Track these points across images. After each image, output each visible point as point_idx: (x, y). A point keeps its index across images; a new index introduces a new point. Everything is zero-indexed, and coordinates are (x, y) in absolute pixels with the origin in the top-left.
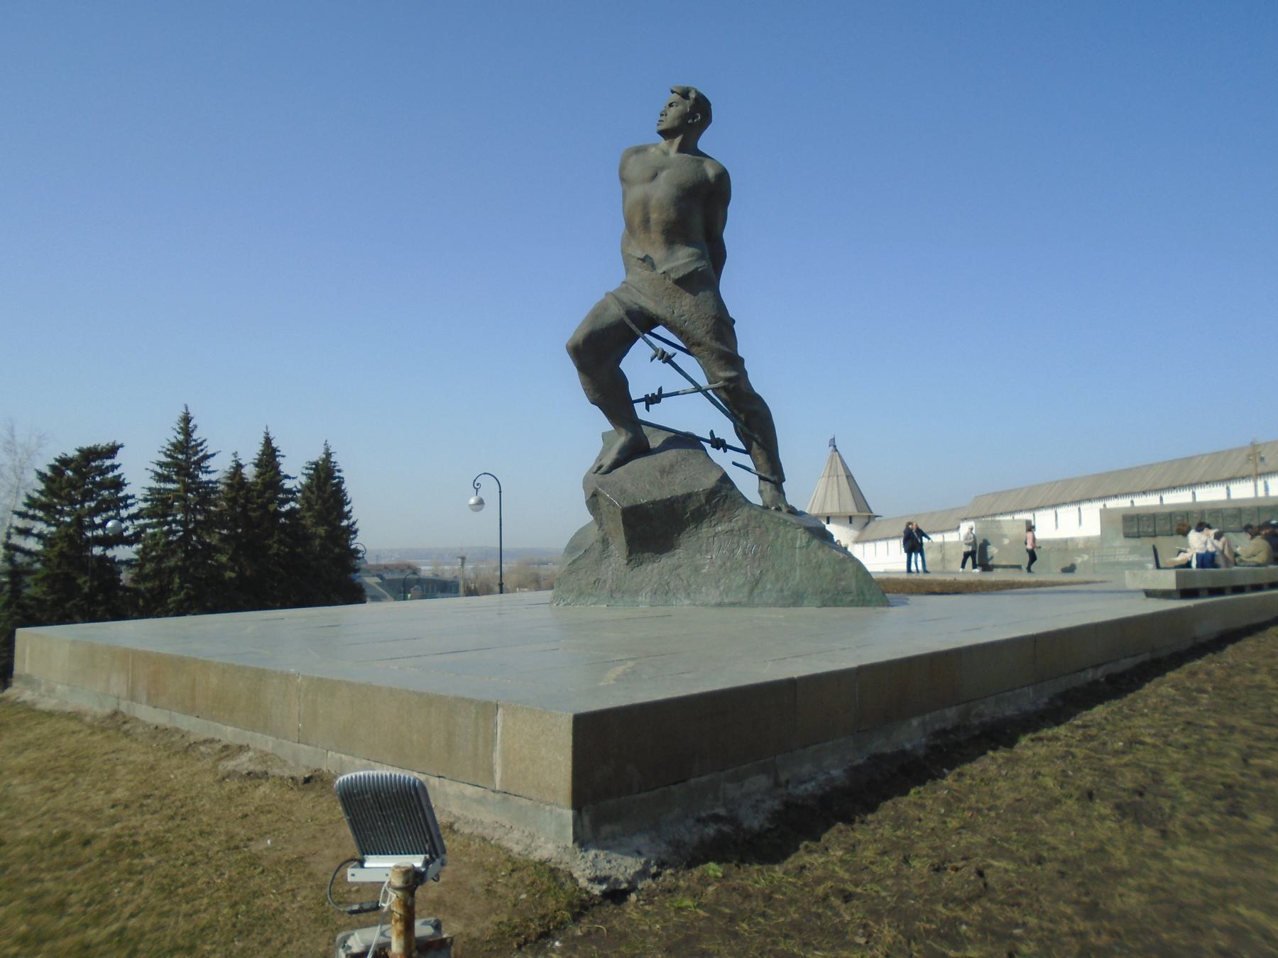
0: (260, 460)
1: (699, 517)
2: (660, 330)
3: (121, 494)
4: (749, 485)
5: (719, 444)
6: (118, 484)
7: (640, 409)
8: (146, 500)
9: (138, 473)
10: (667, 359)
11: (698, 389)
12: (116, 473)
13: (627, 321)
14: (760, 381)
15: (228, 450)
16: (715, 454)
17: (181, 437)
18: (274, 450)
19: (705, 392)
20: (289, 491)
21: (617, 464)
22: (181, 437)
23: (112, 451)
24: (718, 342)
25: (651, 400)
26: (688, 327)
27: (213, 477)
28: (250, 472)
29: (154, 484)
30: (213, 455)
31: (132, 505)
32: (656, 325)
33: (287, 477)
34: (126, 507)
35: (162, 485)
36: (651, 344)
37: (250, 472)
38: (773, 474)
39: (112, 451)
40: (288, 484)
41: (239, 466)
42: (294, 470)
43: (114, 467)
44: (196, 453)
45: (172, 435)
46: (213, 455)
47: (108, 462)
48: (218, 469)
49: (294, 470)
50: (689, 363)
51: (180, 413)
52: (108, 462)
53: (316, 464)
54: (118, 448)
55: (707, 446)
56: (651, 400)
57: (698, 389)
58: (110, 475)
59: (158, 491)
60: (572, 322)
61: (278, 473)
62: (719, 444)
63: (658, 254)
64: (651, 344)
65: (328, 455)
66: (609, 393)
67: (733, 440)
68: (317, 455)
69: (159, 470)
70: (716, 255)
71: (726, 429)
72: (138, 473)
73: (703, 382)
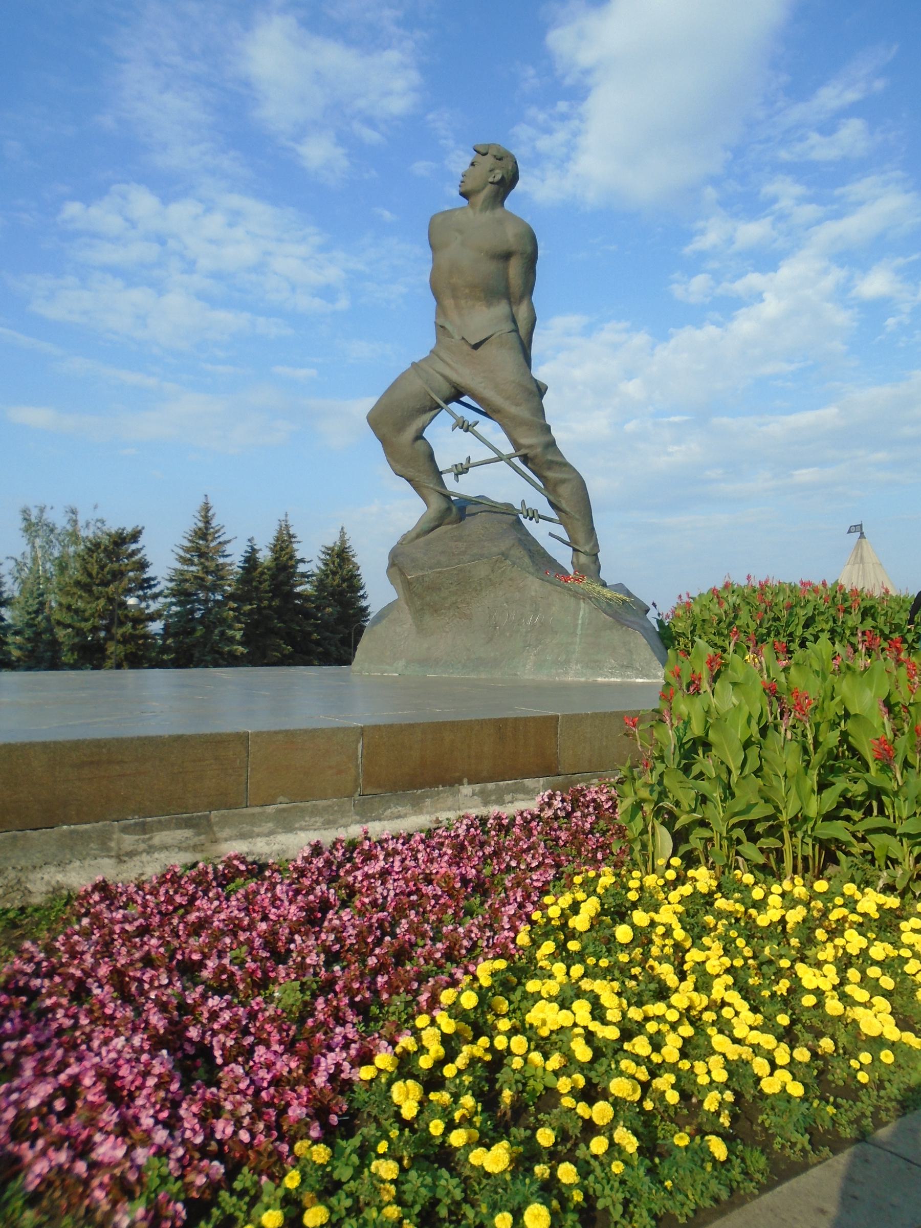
0: (275, 546)
2: (466, 399)
3: (145, 576)
5: (533, 515)
6: (143, 566)
8: (171, 580)
9: (163, 558)
11: (500, 458)
12: (140, 556)
13: (429, 390)
15: (245, 535)
17: (201, 525)
18: (291, 536)
19: (508, 459)
20: (304, 575)
21: (418, 536)
22: (201, 525)
23: (135, 536)
25: (461, 470)
26: (489, 394)
27: (228, 560)
28: (265, 556)
29: (178, 566)
30: (229, 541)
31: (155, 585)
32: (462, 395)
33: (302, 561)
34: (150, 587)
35: (186, 568)
36: (452, 414)
37: (265, 556)
39: (135, 536)
40: (301, 568)
41: (254, 551)
42: (310, 556)
43: (139, 550)
44: (215, 538)
45: (192, 522)
46: (229, 541)
47: (133, 547)
48: (235, 557)
49: (310, 556)
51: (199, 503)
52: (133, 547)
53: (332, 549)
54: (140, 532)
55: (521, 516)
56: (461, 470)
58: (136, 558)
59: (182, 573)
61: (292, 557)
62: (533, 515)
64: (452, 414)
65: (343, 542)
66: (417, 465)
68: (332, 540)
69: (182, 554)
72: (163, 558)
73: (507, 449)
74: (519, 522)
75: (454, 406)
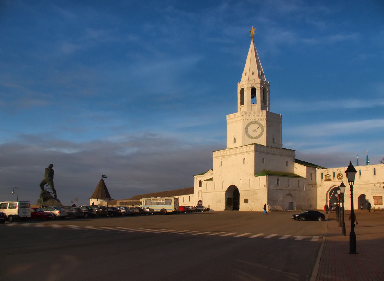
1: (49, 199)
4: (54, 197)
5: (51, 193)
7: (45, 190)
10: (48, 186)
11: (50, 189)
14: (55, 188)
16: (51, 194)
24: (52, 184)
38: (56, 196)
50: (49, 186)
57: (50, 189)
60: (40, 182)
63: (48, 177)
67: (53, 193)
70: (52, 178)
71: (52, 192)
74: (50, 194)
75: (46, 184)
